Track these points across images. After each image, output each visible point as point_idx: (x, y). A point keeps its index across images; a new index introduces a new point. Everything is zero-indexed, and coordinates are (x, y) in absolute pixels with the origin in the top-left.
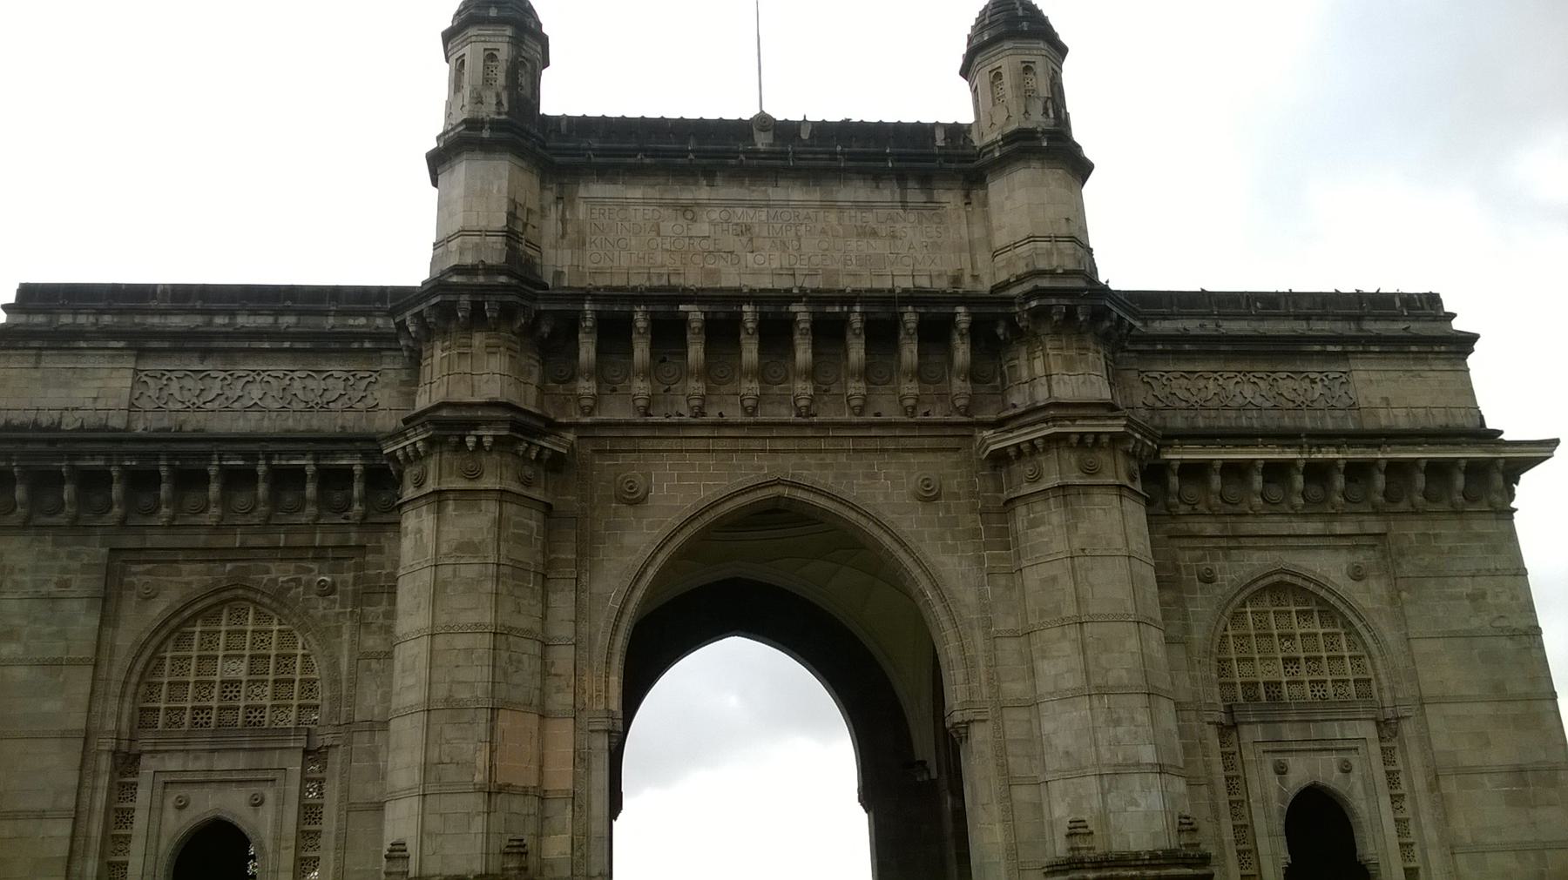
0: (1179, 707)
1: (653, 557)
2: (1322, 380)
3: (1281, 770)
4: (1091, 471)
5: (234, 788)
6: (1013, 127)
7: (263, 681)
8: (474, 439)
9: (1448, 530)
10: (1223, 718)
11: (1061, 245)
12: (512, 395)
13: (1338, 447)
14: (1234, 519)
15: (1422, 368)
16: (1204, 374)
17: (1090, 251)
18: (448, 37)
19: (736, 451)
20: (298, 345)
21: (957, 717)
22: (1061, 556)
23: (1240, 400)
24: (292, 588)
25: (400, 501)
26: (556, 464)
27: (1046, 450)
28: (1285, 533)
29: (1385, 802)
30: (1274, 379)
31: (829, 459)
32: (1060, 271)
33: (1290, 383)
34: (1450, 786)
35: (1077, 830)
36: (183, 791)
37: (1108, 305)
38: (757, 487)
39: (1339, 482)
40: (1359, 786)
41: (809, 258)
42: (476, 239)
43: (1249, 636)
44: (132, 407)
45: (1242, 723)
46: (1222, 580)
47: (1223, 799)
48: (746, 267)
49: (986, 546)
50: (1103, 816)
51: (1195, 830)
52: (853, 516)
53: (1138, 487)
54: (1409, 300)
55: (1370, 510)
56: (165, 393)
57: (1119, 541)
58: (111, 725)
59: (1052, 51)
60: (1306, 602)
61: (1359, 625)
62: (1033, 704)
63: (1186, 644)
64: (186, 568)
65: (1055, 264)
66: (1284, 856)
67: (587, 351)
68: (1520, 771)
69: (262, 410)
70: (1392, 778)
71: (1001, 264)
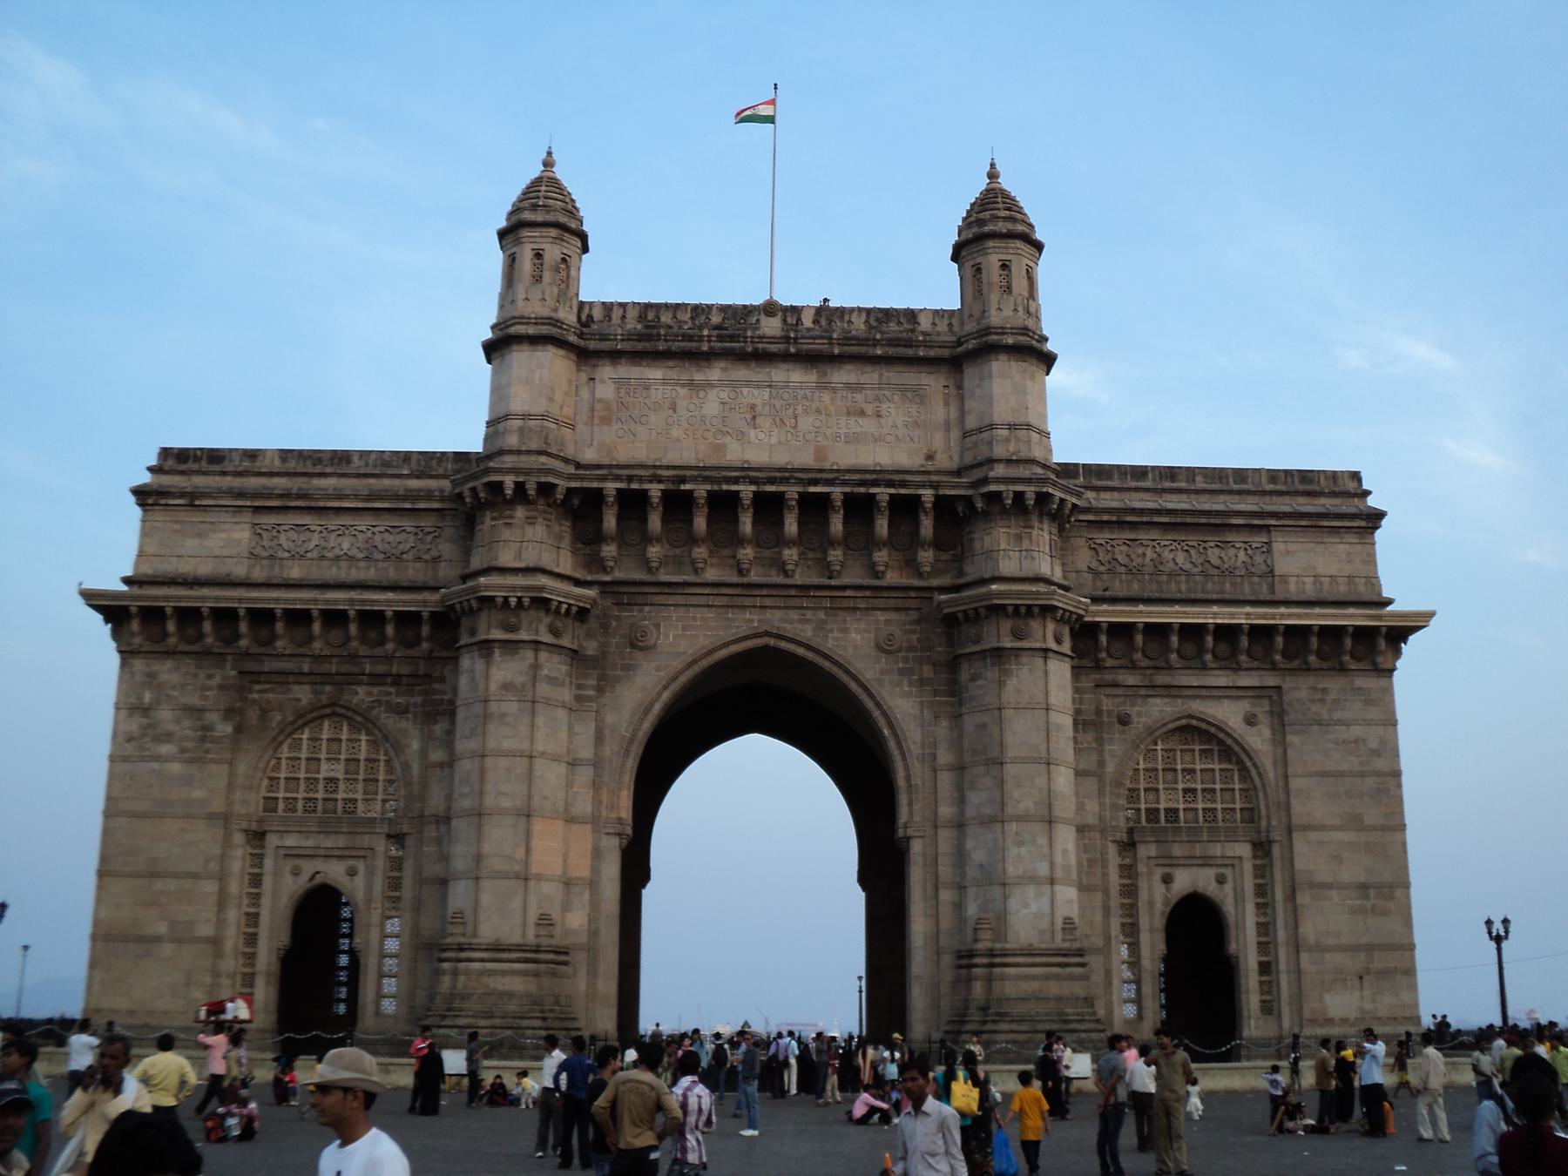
0: (1081, 829)
1: (659, 694)
2: (1246, 549)
3: (1167, 880)
4: (1018, 636)
5: (335, 861)
7: (355, 780)
8: (515, 599)
9: (1334, 685)
12: (547, 560)
14: (1152, 671)
15: (1334, 540)
16: (1145, 543)
17: (1047, 435)
18: (502, 234)
19: (732, 607)
20: (378, 505)
22: (991, 707)
24: (374, 708)
25: (457, 645)
26: (582, 614)
27: (987, 617)
28: (1196, 684)
29: (1250, 909)
30: (1204, 548)
31: (809, 614)
32: (1014, 458)
33: (1217, 551)
34: (1303, 898)
36: (297, 862)
37: (1051, 491)
38: (747, 638)
39: (1244, 641)
40: (1231, 895)
41: (804, 436)
42: (520, 423)
43: (1156, 770)
44: (253, 555)
45: (1139, 842)
46: (1138, 723)
47: (1116, 901)
48: (749, 442)
49: (936, 693)
50: (1002, 918)
51: (1075, 929)
52: (826, 664)
53: (1066, 648)
54: (1334, 476)
55: (1269, 667)
56: (274, 543)
57: (1040, 697)
59: (1032, 250)
60: (1209, 742)
61: (1249, 764)
62: (960, 825)
63: (1100, 778)
64: (296, 688)
65: (1012, 449)
66: (1161, 947)
67: (610, 521)
68: (1364, 888)
69: (351, 559)
70: (1261, 891)
71: (969, 445)
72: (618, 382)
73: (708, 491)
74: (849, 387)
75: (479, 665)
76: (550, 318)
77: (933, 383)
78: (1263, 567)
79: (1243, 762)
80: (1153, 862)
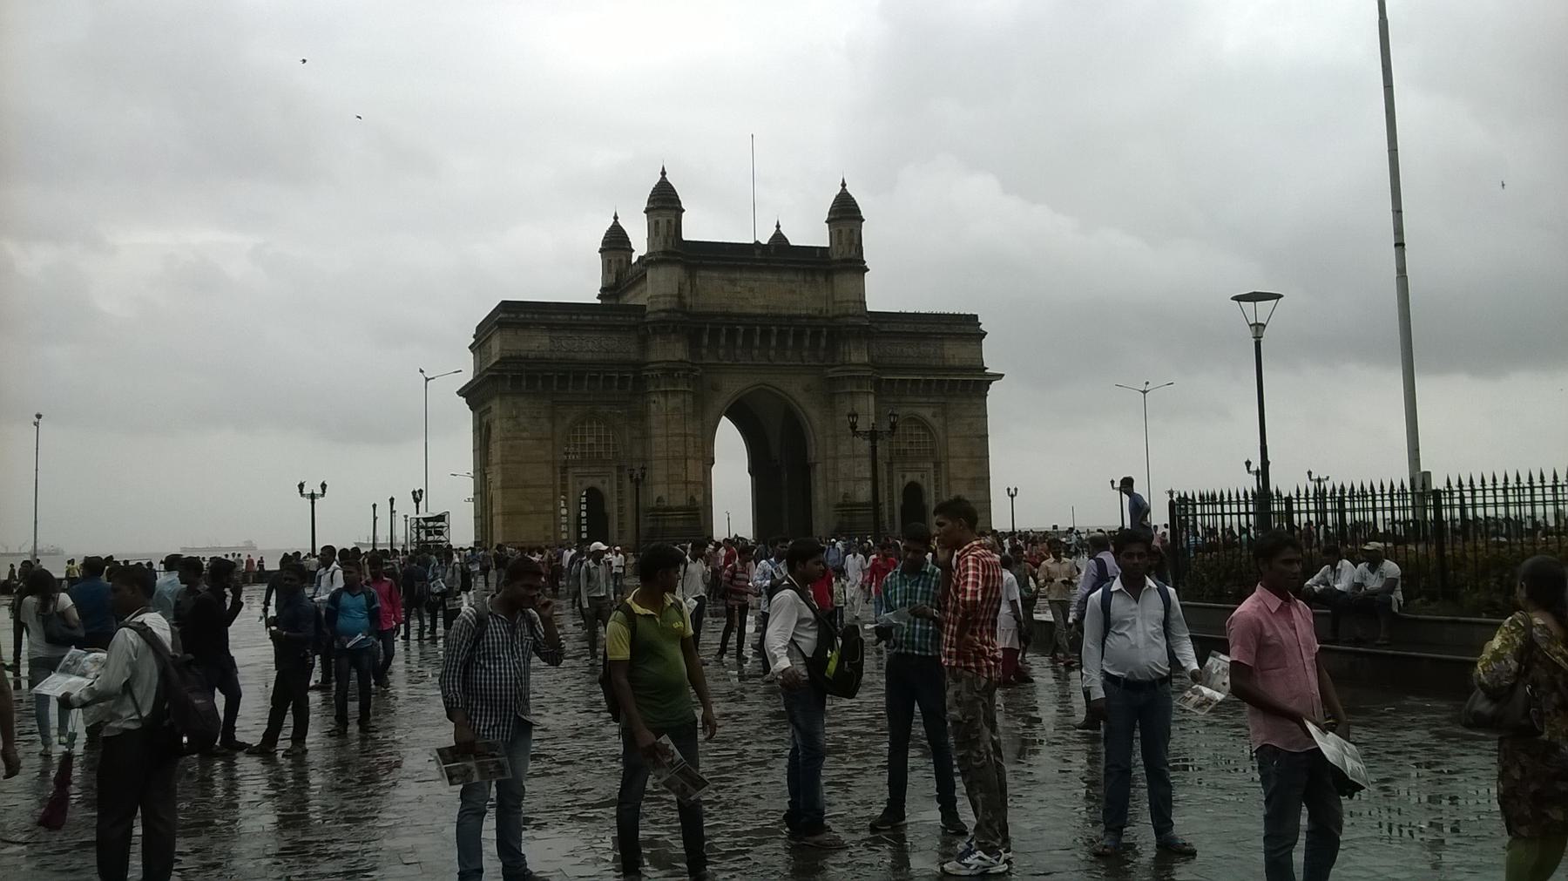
3: (904, 477)
6: (844, 256)
10: (888, 461)
13: (935, 375)
21: (813, 461)
29: (933, 487)
34: (952, 483)
35: (846, 495)
53: (872, 391)
67: (706, 340)
68: (973, 479)
70: (936, 480)
75: (662, 400)
77: (821, 279)
79: (929, 431)
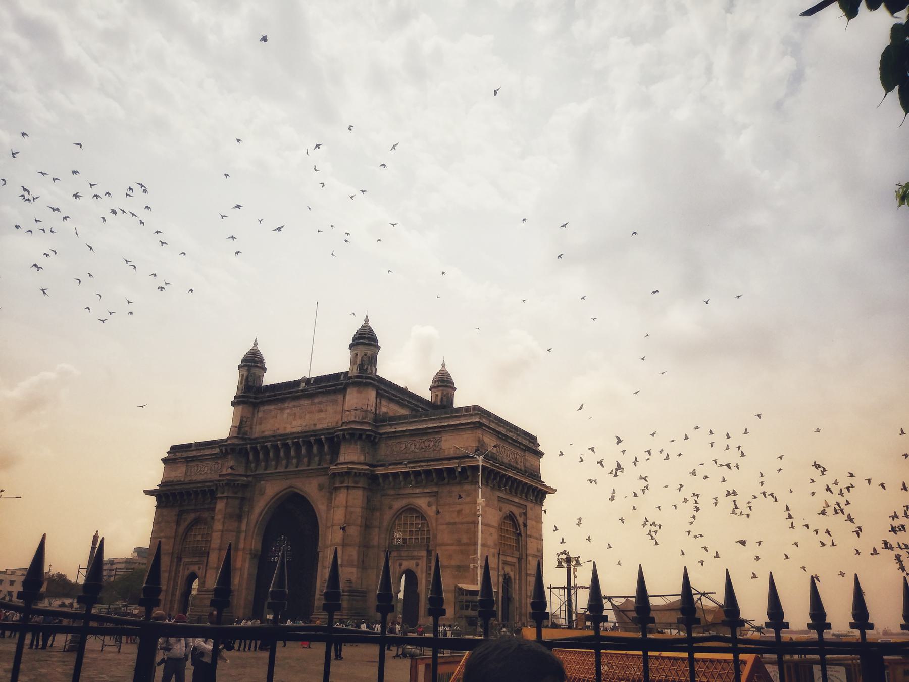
3: (401, 565)
11: (352, 412)
23: (411, 450)
26: (245, 486)
28: (411, 492)
29: (424, 575)
57: (344, 503)
58: (177, 552)
67: (251, 457)
68: (458, 567)
72: (264, 411)
73: (271, 444)
74: (320, 403)
76: (242, 395)
77: (340, 397)
78: (440, 447)
80: (396, 558)
